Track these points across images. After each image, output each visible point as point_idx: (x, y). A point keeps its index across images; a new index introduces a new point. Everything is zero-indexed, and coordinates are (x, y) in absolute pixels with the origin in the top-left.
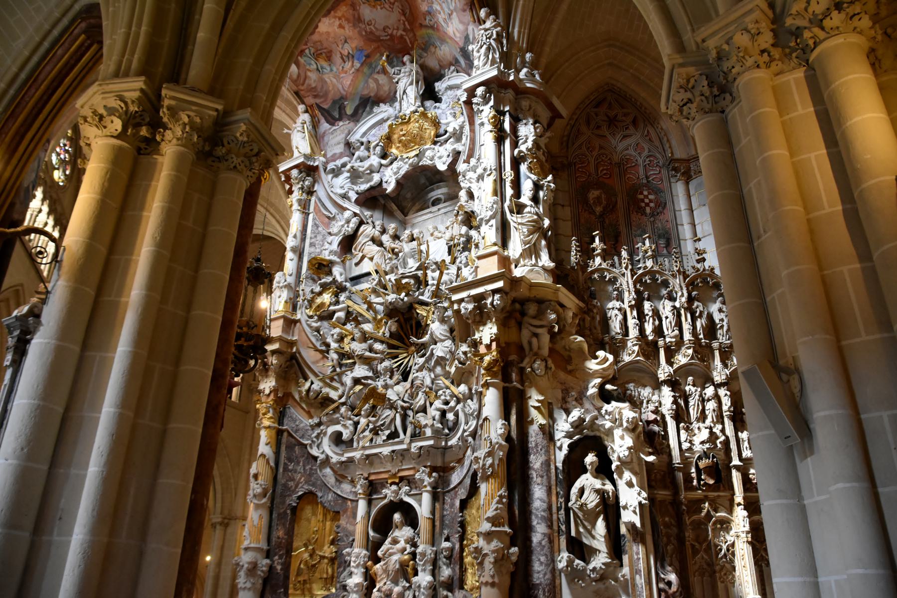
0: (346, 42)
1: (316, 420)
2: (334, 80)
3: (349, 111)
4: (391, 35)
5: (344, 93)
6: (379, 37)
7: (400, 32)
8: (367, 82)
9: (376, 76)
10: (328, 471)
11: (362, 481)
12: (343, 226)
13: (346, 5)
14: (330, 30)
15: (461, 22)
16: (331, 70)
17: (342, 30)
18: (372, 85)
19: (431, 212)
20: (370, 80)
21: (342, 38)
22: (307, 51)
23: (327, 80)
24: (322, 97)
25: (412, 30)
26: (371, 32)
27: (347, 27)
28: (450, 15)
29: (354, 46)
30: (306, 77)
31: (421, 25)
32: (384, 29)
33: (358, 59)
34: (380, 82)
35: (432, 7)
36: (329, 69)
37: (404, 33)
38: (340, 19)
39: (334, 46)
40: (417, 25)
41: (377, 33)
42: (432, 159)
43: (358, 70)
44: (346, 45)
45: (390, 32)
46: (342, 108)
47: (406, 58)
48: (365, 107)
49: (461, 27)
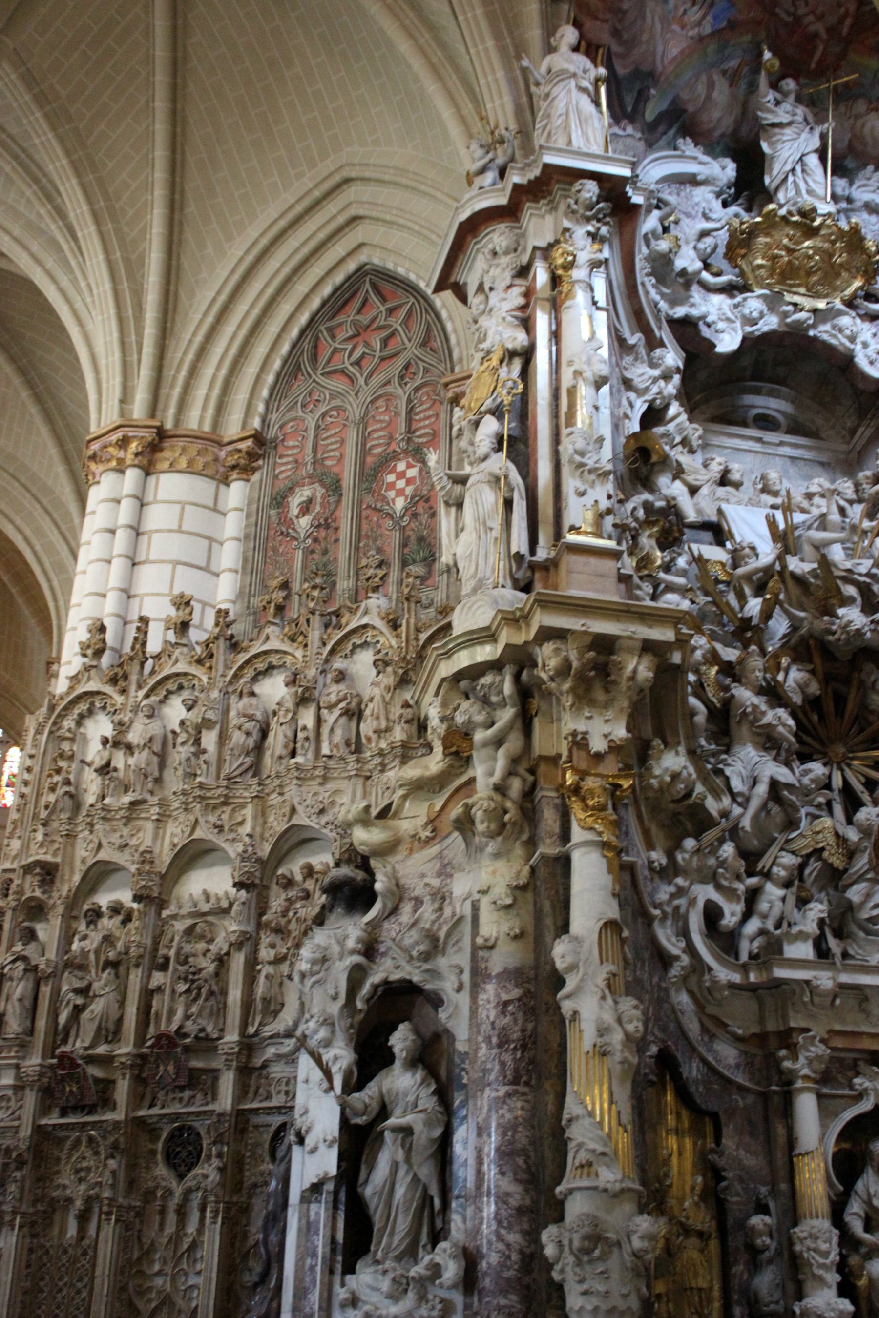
1: (658, 857)
2: (658, 26)
3: (650, 113)
4: (798, 20)
5: (660, 69)
7: (819, 28)
8: (697, 76)
10: (683, 999)
11: (819, 1049)
12: (655, 380)
18: (701, 89)
19: (759, 440)
20: (704, 78)
24: (621, 42)
33: (715, 18)
34: (715, 94)
37: (824, 35)
42: (852, 339)
43: (701, 39)
45: (801, 11)
46: (642, 98)
47: (790, 84)
48: (670, 127)
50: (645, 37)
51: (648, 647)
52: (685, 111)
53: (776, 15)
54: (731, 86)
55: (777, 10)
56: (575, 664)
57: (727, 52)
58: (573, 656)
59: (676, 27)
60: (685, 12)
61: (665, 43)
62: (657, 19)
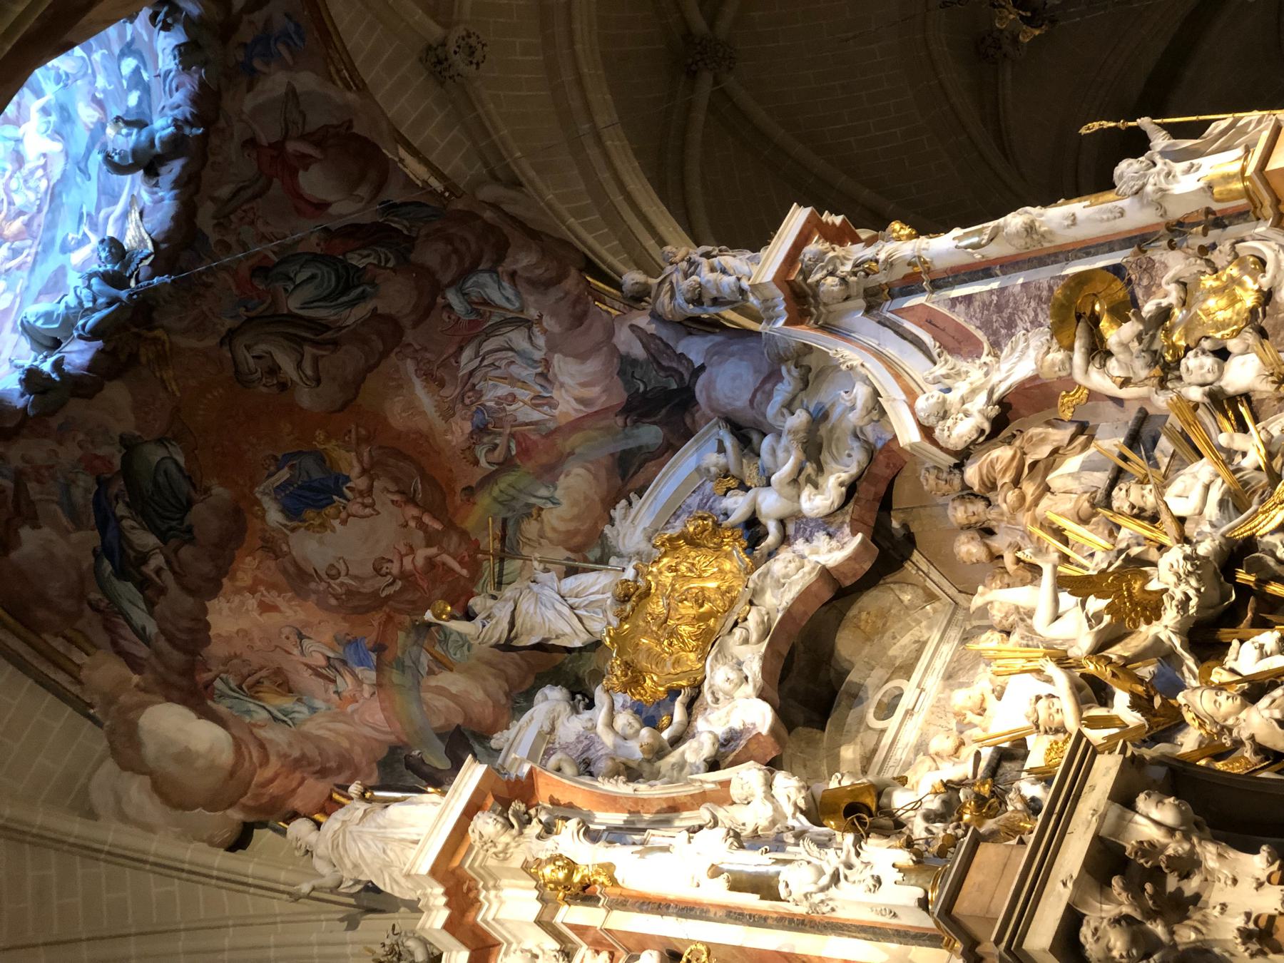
0: (301, 637)
2: (341, 727)
4: (403, 575)
5: (392, 738)
6: (375, 594)
7: (422, 554)
8: (420, 701)
9: (433, 682)
13: (251, 553)
14: (244, 624)
15: (582, 357)
16: (313, 710)
17: (275, 617)
18: (440, 703)
19: (909, 713)
21: (286, 631)
22: (218, 684)
23: (321, 732)
24: (340, 769)
25: (450, 526)
26: (350, 593)
27: (280, 602)
28: (545, 377)
29: (328, 638)
30: (262, 745)
31: (470, 491)
32: (377, 571)
34: (454, 690)
35: (482, 409)
36: (305, 710)
37: (434, 550)
38: (252, 590)
39: (279, 659)
40: (458, 499)
41: (367, 588)
43: (379, 685)
44: (306, 642)
45: (395, 569)
49: (593, 366)
50: (346, 744)
51: (1124, 797)
52: (458, 726)
53: (388, 597)
54: (451, 670)
55: (383, 595)
56: (1126, 909)
57: (408, 662)
58: (1110, 910)
59: (350, 709)
60: (336, 692)
61: (366, 724)
62: (331, 725)
